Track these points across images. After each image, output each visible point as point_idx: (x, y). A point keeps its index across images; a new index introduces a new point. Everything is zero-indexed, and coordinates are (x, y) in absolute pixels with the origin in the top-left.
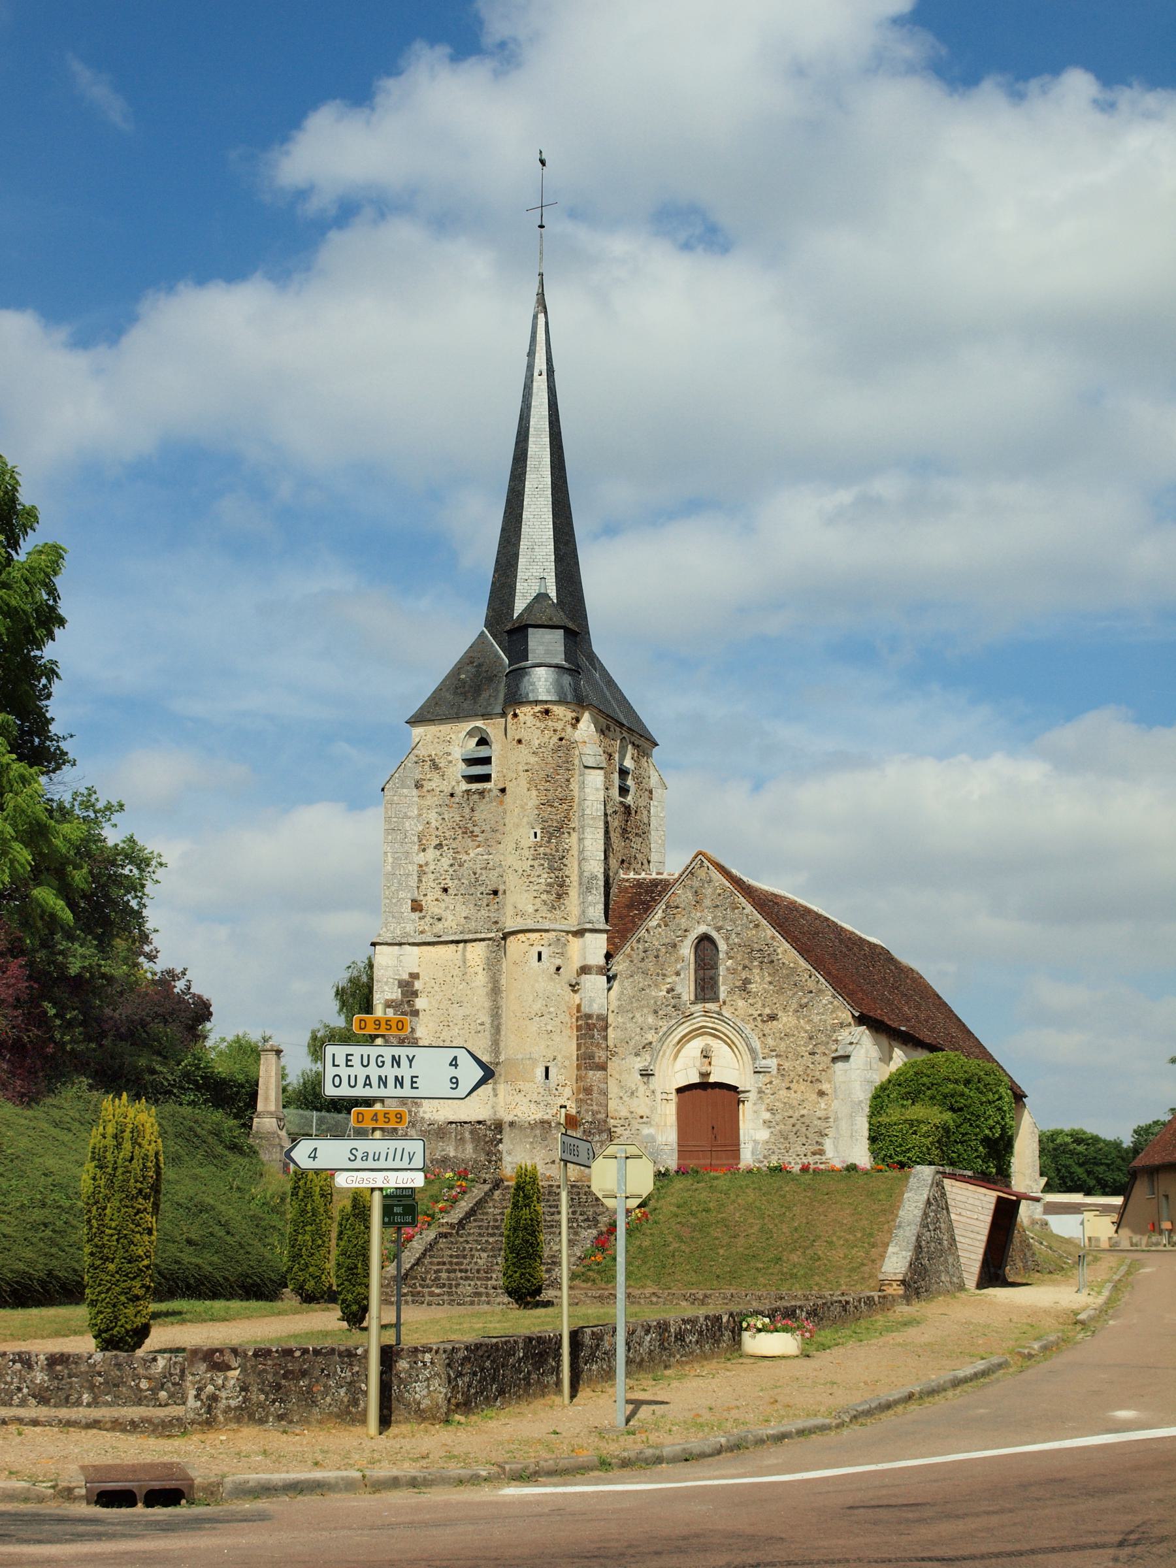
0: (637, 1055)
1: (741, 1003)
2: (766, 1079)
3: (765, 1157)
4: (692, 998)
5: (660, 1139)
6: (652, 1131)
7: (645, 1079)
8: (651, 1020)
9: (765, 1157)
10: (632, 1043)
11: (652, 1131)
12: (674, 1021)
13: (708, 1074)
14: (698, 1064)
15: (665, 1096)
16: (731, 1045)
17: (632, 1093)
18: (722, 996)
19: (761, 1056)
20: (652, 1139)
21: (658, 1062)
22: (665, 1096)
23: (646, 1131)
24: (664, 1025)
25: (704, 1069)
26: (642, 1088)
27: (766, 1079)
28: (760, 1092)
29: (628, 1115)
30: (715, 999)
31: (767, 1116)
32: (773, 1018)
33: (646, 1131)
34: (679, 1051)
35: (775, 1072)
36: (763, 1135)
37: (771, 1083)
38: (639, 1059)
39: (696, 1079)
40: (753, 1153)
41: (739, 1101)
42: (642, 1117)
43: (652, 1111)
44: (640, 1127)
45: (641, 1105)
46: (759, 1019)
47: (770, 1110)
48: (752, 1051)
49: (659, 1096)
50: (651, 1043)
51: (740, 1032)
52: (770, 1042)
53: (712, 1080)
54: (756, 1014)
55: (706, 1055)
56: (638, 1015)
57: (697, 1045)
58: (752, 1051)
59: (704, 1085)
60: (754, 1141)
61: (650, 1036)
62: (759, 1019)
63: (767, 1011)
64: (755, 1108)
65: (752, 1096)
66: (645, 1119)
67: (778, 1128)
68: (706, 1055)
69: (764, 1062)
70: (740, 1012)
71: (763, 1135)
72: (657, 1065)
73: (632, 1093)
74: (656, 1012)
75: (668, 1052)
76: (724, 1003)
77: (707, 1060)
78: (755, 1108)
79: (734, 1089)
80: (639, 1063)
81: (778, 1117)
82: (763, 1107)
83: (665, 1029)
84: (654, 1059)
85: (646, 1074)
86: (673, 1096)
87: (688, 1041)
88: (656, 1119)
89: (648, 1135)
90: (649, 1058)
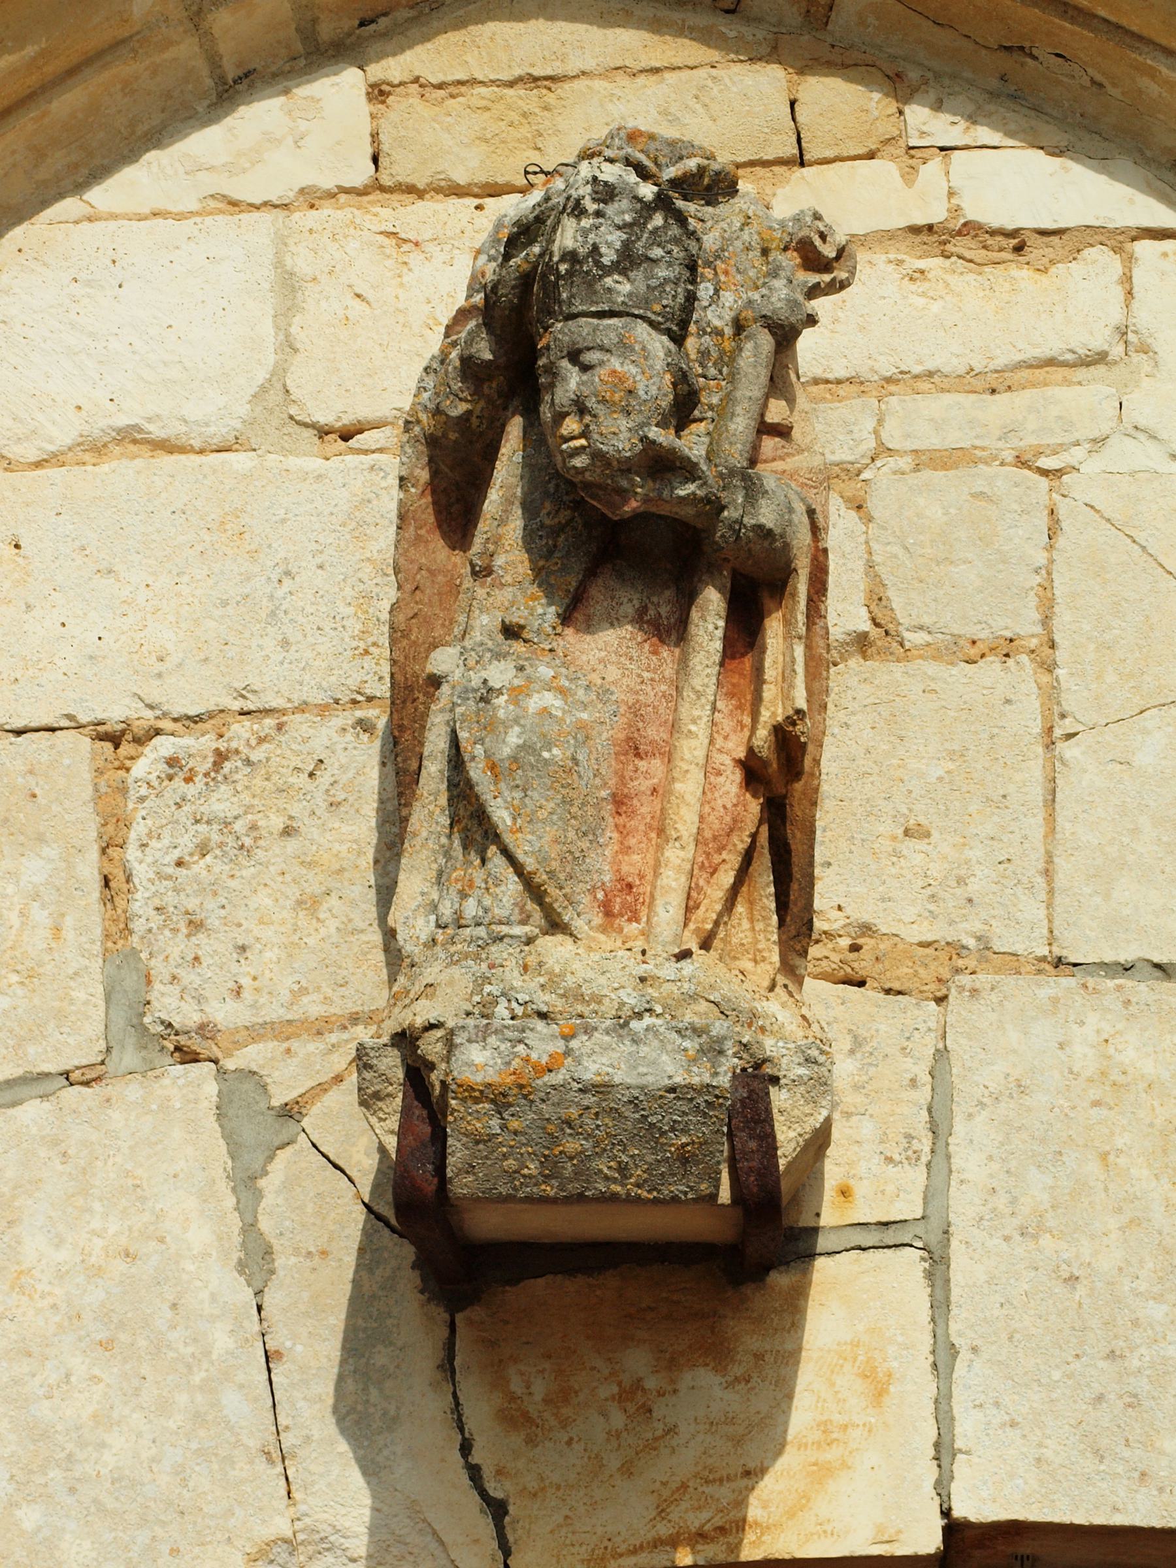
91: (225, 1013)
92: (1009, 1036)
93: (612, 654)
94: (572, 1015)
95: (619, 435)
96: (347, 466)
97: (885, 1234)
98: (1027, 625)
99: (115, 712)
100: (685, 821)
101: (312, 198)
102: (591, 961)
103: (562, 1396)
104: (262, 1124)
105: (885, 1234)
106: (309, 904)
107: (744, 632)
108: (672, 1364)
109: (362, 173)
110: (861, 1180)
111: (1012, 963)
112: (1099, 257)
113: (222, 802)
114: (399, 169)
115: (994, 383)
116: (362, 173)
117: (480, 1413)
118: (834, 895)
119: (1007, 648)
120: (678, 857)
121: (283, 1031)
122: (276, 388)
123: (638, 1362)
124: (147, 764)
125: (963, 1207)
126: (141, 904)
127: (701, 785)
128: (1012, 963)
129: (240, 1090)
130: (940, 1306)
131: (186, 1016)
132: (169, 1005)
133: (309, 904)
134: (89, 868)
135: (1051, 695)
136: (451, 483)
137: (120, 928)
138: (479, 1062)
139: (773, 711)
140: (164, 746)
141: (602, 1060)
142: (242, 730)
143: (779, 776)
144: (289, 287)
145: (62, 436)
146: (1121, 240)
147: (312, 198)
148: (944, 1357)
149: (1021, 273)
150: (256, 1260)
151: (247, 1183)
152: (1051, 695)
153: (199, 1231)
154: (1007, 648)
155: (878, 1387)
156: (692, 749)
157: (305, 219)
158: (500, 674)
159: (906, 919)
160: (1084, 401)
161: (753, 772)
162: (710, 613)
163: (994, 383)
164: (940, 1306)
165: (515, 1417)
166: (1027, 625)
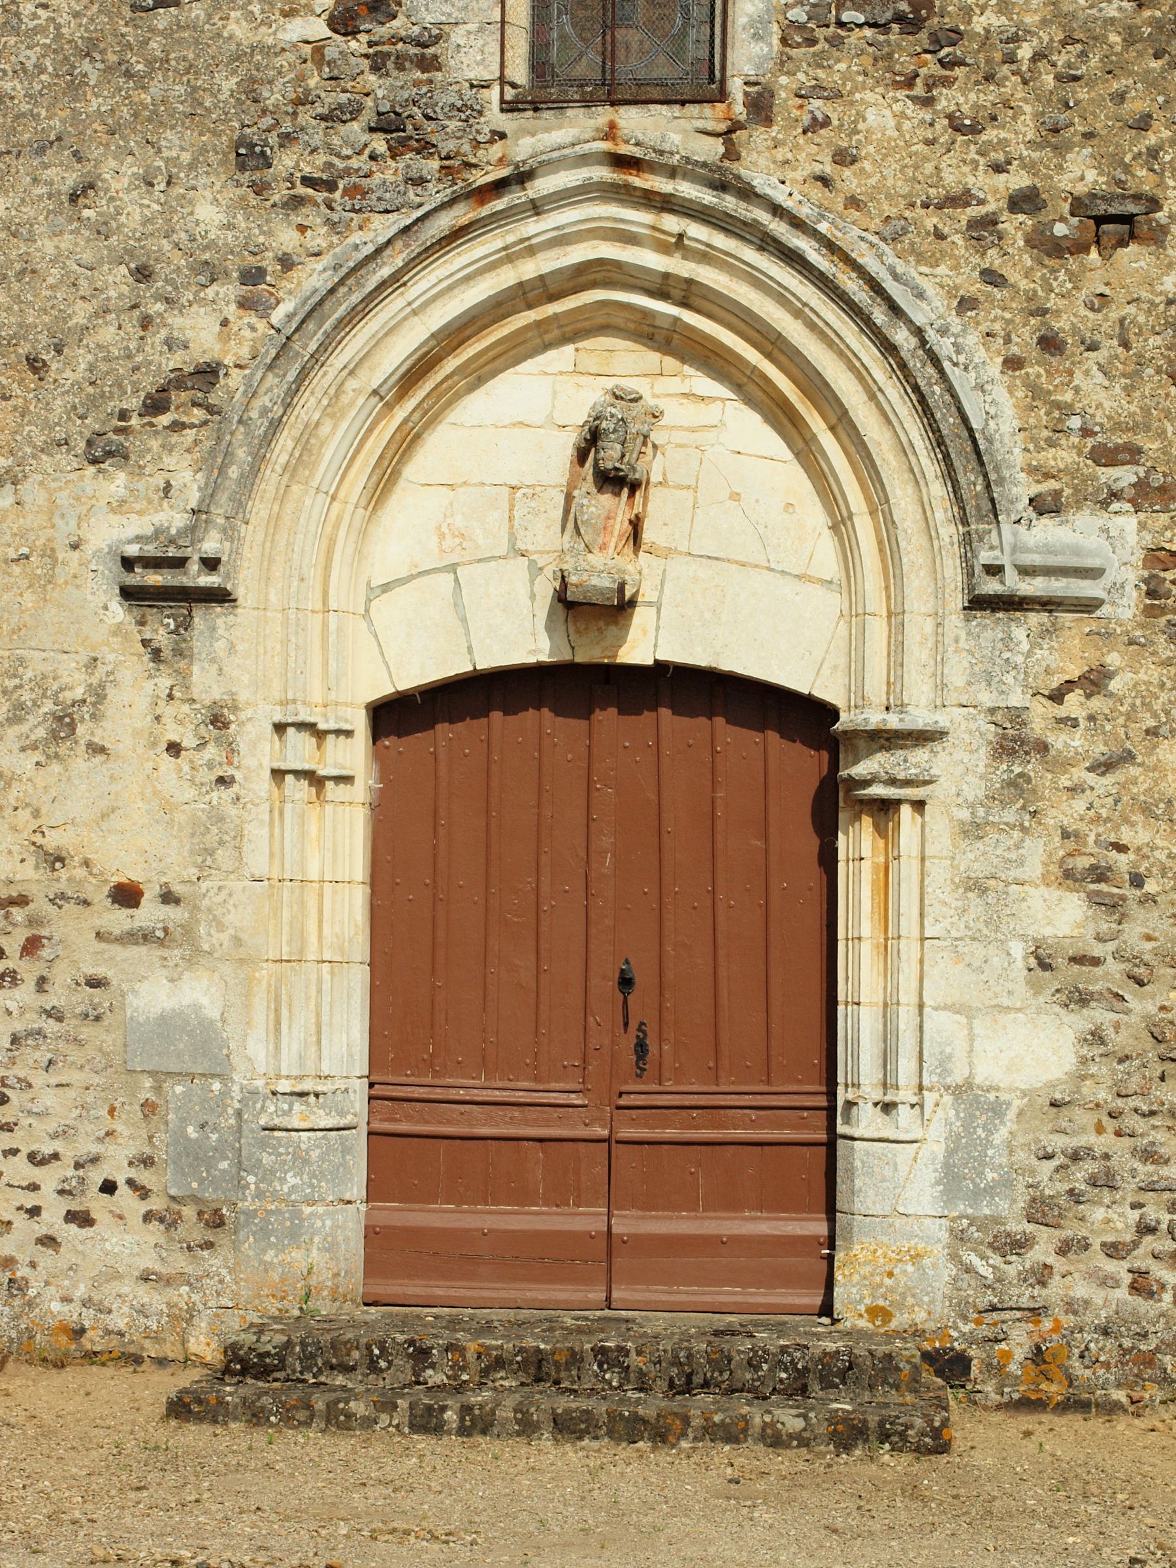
0: (103, 453)
1: (882, 115)
2: (1065, 655)
3: (1041, 1211)
4: (519, 72)
5: (257, 1057)
6: (198, 993)
7: (160, 632)
8: (211, 210)
9: (1041, 1211)
10: (73, 370)
11: (198, 993)
12: (383, 227)
13: (618, 608)
14: (544, 534)
15: (300, 751)
16: (792, 407)
17: (64, 724)
18: (748, 57)
19: (1021, 489)
20: (198, 1051)
21: (260, 508)
22: (300, 751)
23: (155, 992)
24: (313, 254)
25: (597, 572)
26: (135, 692)
27: (1065, 655)
28: (1013, 742)
29: (31, 876)
30: (708, 87)
31: (1066, 917)
32: (1116, 222)
33: (155, 992)
34: (407, 442)
35: (1126, 608)
36: (1032, 1050)
37: (1094, 681)
38: (118, 482)
39: (521, 637)
40: (952, 1180)
41: (831, 804)
42: (127, 895)
43: (204, 871)
44: (115, 963)
45: (123, 811)
46: (1015, 226)
47: (1089, 877)
48: (960, 450)
49: (258, 751)
50: (208, 373)
51: (873, 311)
52: (1097, 392)
53: (639, 647)
54: (994, 190)
55: (608, 464)
56: (118, 176)
57: (536, 406)
58: (960, 450)
59: (585, 682)
60: (962, 1091)
61: (205, 328)
62: (1015, 226)
63: (1081, 173)
64: (975, 859)
65: (958, 772)
66: (149, 913)
67: (1142, 1005)
68: (608, 464)
69: (1046, 535)
70: (880, 175)
71: (1032, 1050)
72: (253, 534)
73: (64, 724)
74: (250, 157)
75: (335, 441)
76: (761, 107)
77: (610, 509)
78: (975, 859)
79: (803, 718)
80: (117, 515)
81: (1142, 929)
82: (1037, 854)
83: (313, 277)
84: (229, 489)
85: (170, 590)
86: (354, 755)
87: (479, 374)
88: (234, 907)
89: (168, 1025)
90: (190, 486)
91: (531, 548)
92: (678, 568)
93: (606, 499)
94: (592, 571)
95: (610, 465)
96: (563, 434)
97: (650, 604)
98: (693, 483)
99: (514, 483)
100: (616, 533)
101: (561, 373)
102: (596, 559)
103: (586, 629)
104: (535, 570)
105: (650, 604)
106: (548, 527)
107: (632, 494)
108: (607, 624)
109: (572, 368)
110: (647, 593)
111: (681, 553)
112: (719, 403)
113: (533, 504)
114: (579, 369)
115: (693, 430)
116: (572, 368)
117: (571, 630)
118: (647, 535)
119: (689, 487)
120: (614, 540)
121: (541, 552)
122: (550, 416)
123: (601, 623)
124: (519, 494)
125: (665, 600)
126: (516, 523)
127: (620, 524)
128: (681, 553)
129: (532, 563)
130: (658, 618)
131: (523, 547)
132: (520, 545)
133: (548, 527)
134: (507, 515)
135: (696, 498)
136: (581, 456)
137: (511, 527)
138: (573, 579)
139: (635, 511)
140: (522, 491)
141: (595, 581)
142: (538, 489)
143: (636, 525)
144: (555, 393)
145: (507, 422)
146: (723, 400)
147: (561, 373)
148: (658, 628)
149: (702, 405)
150: (533, 597)
151: (532, 582)
152: (696, 498)
153: (523, 590)
154: (689, 487)
155: (645, 633)
156: (619, 519)
157: (559, 378)
158: (585, 502)
159: (662, 542)
160: (711, 435)
161: (631, 522)
162: (626, 491)
163: (693, 430)
164: (658, 618)
165: (578, 632)
166: (693, 483)
